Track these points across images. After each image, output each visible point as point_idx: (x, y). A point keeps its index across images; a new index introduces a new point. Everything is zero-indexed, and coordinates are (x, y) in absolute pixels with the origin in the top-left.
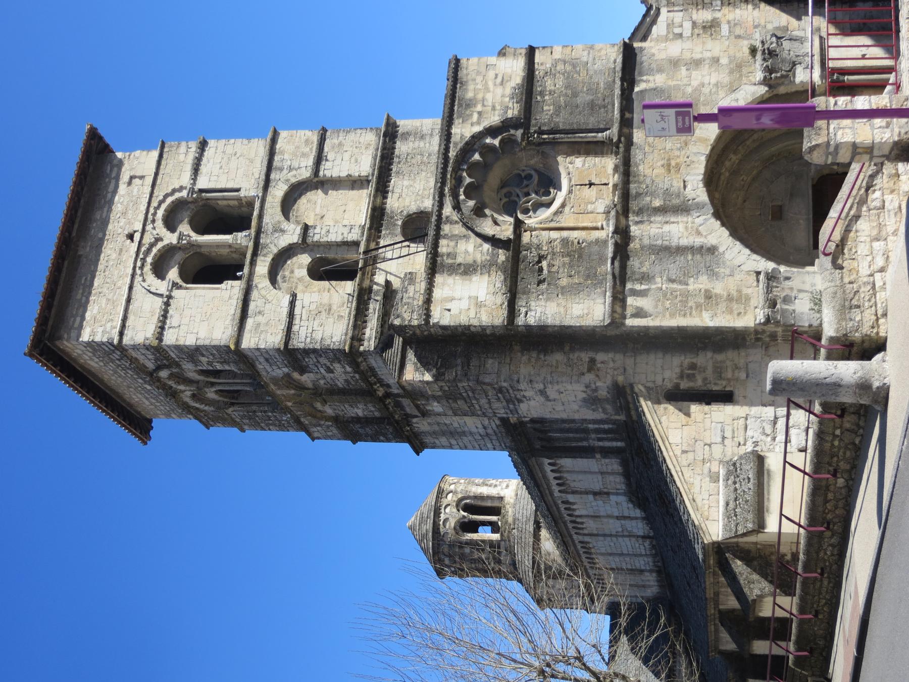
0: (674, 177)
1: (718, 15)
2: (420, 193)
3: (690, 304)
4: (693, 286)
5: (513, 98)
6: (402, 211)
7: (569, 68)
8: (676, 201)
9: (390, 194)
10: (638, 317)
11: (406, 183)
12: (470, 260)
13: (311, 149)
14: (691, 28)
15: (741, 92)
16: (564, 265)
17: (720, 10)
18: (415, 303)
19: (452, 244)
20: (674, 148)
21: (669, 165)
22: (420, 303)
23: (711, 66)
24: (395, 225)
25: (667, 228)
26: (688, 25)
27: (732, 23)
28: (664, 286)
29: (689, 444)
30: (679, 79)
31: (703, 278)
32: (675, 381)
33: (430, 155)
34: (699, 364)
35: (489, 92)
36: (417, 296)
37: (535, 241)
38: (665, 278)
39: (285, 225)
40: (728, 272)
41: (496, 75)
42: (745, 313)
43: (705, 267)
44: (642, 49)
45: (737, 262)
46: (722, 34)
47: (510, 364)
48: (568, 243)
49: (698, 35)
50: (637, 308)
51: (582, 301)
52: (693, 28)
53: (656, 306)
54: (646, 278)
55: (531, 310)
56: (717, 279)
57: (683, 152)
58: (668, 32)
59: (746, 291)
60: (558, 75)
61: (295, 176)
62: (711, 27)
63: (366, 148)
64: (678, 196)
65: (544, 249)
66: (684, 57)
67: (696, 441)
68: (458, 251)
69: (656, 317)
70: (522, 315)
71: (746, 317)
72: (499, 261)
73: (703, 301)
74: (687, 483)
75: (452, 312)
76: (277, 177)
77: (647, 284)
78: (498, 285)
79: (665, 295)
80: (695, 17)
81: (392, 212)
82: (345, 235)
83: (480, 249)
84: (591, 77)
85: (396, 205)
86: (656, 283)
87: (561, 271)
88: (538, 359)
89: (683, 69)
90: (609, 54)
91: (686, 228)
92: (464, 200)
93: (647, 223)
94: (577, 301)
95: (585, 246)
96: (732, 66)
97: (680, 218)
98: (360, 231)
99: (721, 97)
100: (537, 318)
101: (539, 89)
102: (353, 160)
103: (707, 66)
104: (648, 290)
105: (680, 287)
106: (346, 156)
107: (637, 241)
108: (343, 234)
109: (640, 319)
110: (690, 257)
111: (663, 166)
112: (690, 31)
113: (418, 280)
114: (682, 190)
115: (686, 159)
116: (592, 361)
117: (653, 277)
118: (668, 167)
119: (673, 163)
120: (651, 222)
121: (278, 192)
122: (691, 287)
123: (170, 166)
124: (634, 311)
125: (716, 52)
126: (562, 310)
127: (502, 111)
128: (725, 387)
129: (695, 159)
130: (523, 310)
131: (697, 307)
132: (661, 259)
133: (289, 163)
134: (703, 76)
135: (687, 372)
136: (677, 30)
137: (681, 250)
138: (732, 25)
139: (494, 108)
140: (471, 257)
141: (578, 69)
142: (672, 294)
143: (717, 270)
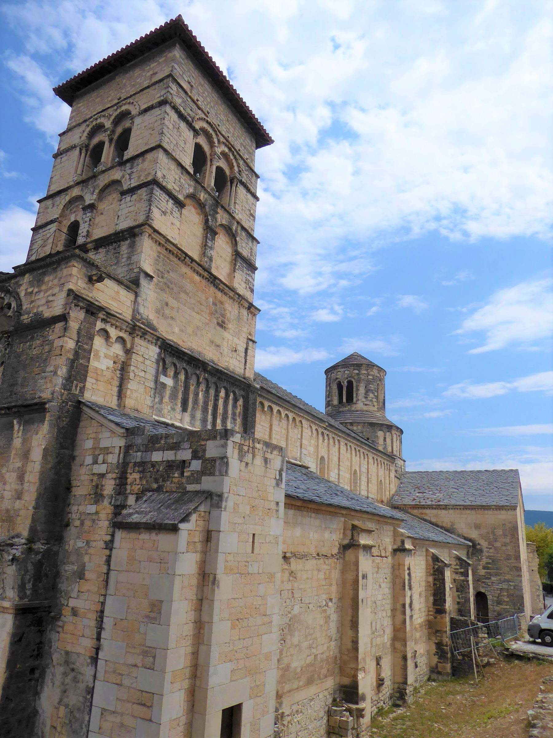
1: (106, 502)
7: (44, 356)
14: (100, 472)
17: (110, 503)
26: (101, 469)
41: (54, 295)
44: (42, 421)
49: (92, 480)
58: (101, 449)
60: (41, 348)
80: (110, 476)
96: (12, 512)
103: (17, 487)
112: (96, 472)
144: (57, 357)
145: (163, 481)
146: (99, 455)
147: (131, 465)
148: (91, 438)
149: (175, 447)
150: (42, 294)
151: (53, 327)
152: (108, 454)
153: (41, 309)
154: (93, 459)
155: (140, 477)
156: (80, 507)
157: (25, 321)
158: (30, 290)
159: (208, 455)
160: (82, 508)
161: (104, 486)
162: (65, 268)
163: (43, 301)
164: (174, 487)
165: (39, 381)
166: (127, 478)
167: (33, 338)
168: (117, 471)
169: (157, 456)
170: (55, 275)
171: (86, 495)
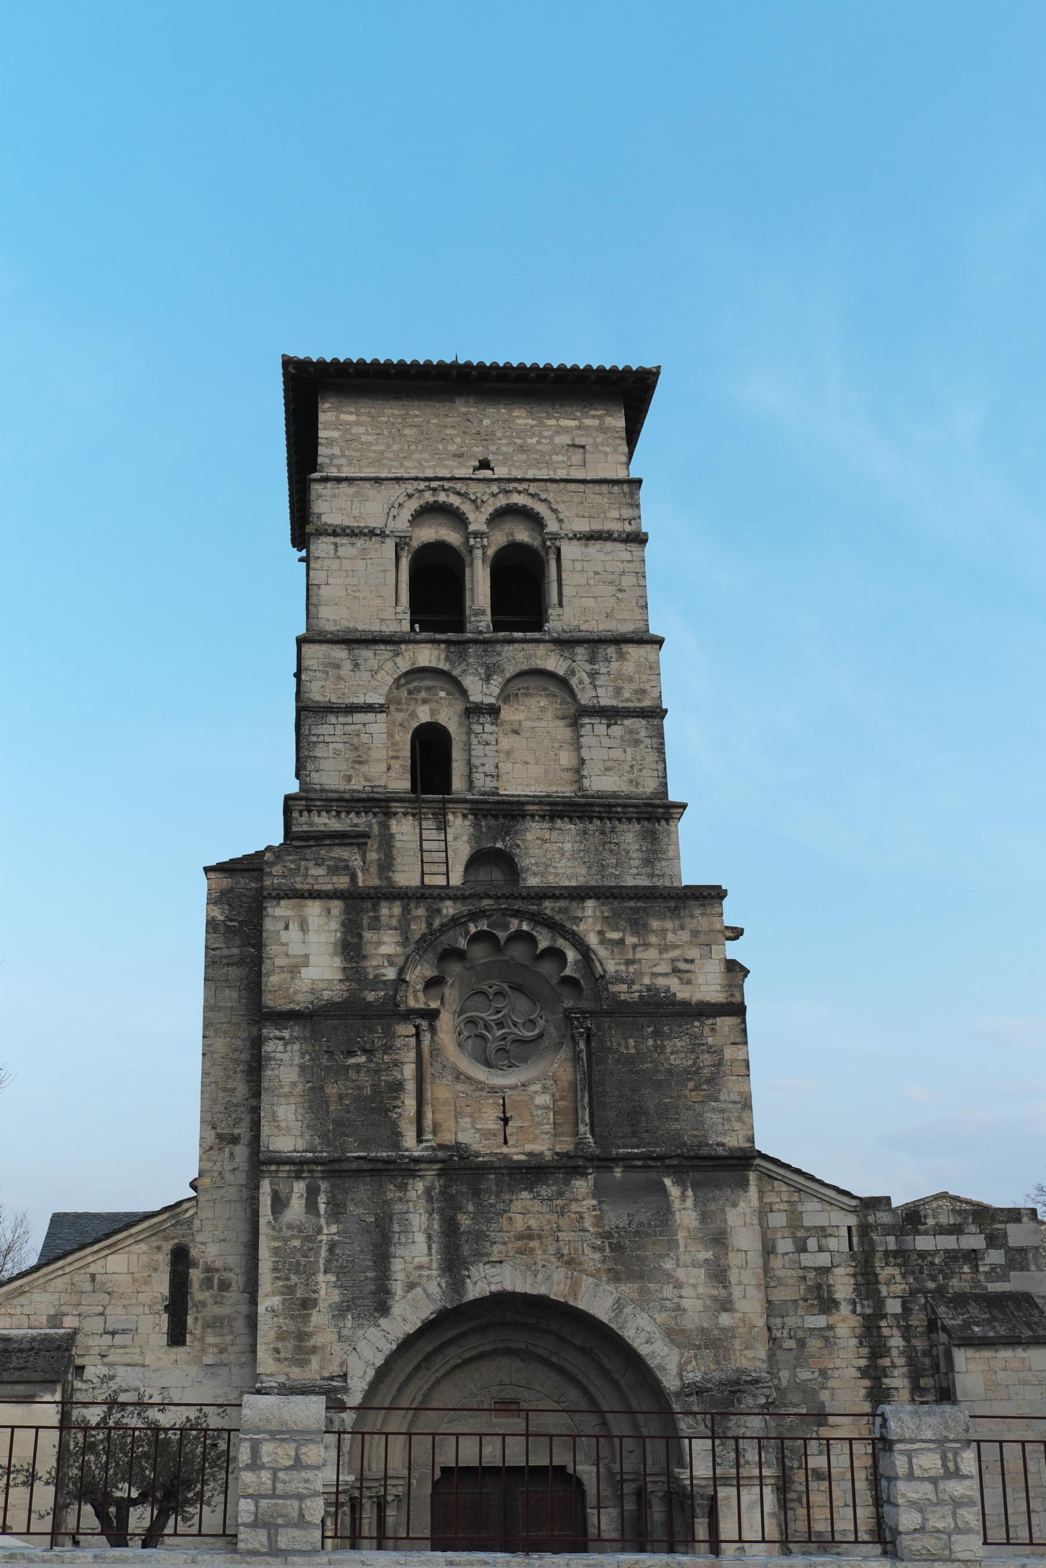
0: (510, 1246)
1: (845, 1309)
2: (551, 870)
3: (293, 1277)
4: (324, 1281)
5: (649, 989)
6: (518, 846)
8: (466, 1250)
9: (547, 825)
10: (272, 1201)
11: (568, 846)
12: (369, 950)
13: (628, 700)
14: (817, 1265)
15: (666, 1349)
16: (360, 1088)
17: (854, 1311)
18: (298, 879)
19: (394, 922)
20: (561, 1244)
21: (531, 1237)
22: (298, 886)
23: (715, 1299)
24: (495, 840)
25: (420, 1238)
26: (823, 1260)
27: (830, 1334)
28: (324, 1237)
29: (104, 1284)
30: (689, 1248)
31: (336, 1297)
32: (201, 1261)
33: (616, 877)
34: (227, 1294)
35: (660, 953)
36: (310, 880)
37: (399, 1043)
38: (336, 1238)
39: (497, 681)
40: (345, 1332)
42: (279, 1360)
43: (354, 1298)
44: (744, 1185)
45: (362, 1345)
46: (806, 1317)
47: (229, 1022)
48: (396, 1091)
49: (804, 1278)
50: (288, 1199)
51: (300, 1117)
52: (816, 1269)
53: (290, 1227)
54: (336, 1211)
55: (285, 1045)
56: (334, 1316)
57: (553, 1259)
58: (808, 1229)
59: (315, 1361)
60: (693, 1057)
61: (581, 682)
62: (819, 1298)
63: (631, 781)
64: (479, 1255)
65: (386, 1057)
66: (730, 1255)
67: (109, 1293)
68: (382, 932)
69: (273, 1228)
70: (278, 1033)
71: (270, 1361)
72: (366, 992)
73: (298, 1295)
74: (46, 1282)
75: (283, 933)
76: (578, 658)
77: (326, 1212)
78: (326, 995)
79: (308, 1239)
81: (516, 833)
82: (481, 769)
83: (386, 964)
84: (689, 1108)
85: (529, 836)
86: (328, 1224)
87: (349, 1084)
88: (236, 1061)
89: (709, 1255)
90: (734, 1134)
91: (420, 1267)
92: (467, 932)
93: (430, 1210)
94: (300, 1111)
95: (390, 1118)
97: (436, 1257)
98: (488, 789)
99: (657, 1316)
100: (272, 1055)
101: (666, 1029)
102: (609, 764)
103: (715, 1292)
104: (317, 1214)
105: (322, 1262)
106: (617, 753)
107: (398, 1194)
108: (483, 765)
109: (269, 1203)
110: (370, 1274)
111: (529, 1228)
113: (335, 879)
114: (486, 1259)
115: (540, 1263)
116: (234, 1140)
117: (337, 1222)
118: (528, 1235)
119: (533, 1244)
120: (431, 1214)
121: (553, 662)
122: (321, 1277)
123: (598, 499)
124: (283, 1196)
125: (740, 1305)
126: (286, 1090)
127: (624, 975)
128: (191, 1333)
129: (540, 1276)
130: (286, 1034)
131: (287, 1287)
132: (367, 1231)
133: (603, 670)
134: (695, 1286)
135: (216, 1276)
136: (812, 1244)
137: (382, 1258)
138: (826, 1335)
139: (629, 962)
140: (373, 951)
141: (705, 1087)
142: (310, 1250)
143: (349, 1317)
144: (740, 1078)
145: (944, 1278)
146: (808, 1238)
147: (879, 1255)
148: (779, 1211)
149: (956, 1230)
150: (652, 954)
151: (710, 1021)
152: (825, 1236)
153: (661, 982)
154: (795, 1244)
155: (901, 1273)
156: (785, 1320)
157: (623, 997)
158: (615, 936)
159: (1012, 1242)
160: (791, 1321)
161: (834, 1286)
162: (703, 914)
163: (664, 968)
164: (965, 1287)
165: (708, 1115)
166: (876, 1275)
167: (657, 1034)
168: (854, 1264)
169: (923, 1243)
170: (677, 923)
171: (796, 1301)
